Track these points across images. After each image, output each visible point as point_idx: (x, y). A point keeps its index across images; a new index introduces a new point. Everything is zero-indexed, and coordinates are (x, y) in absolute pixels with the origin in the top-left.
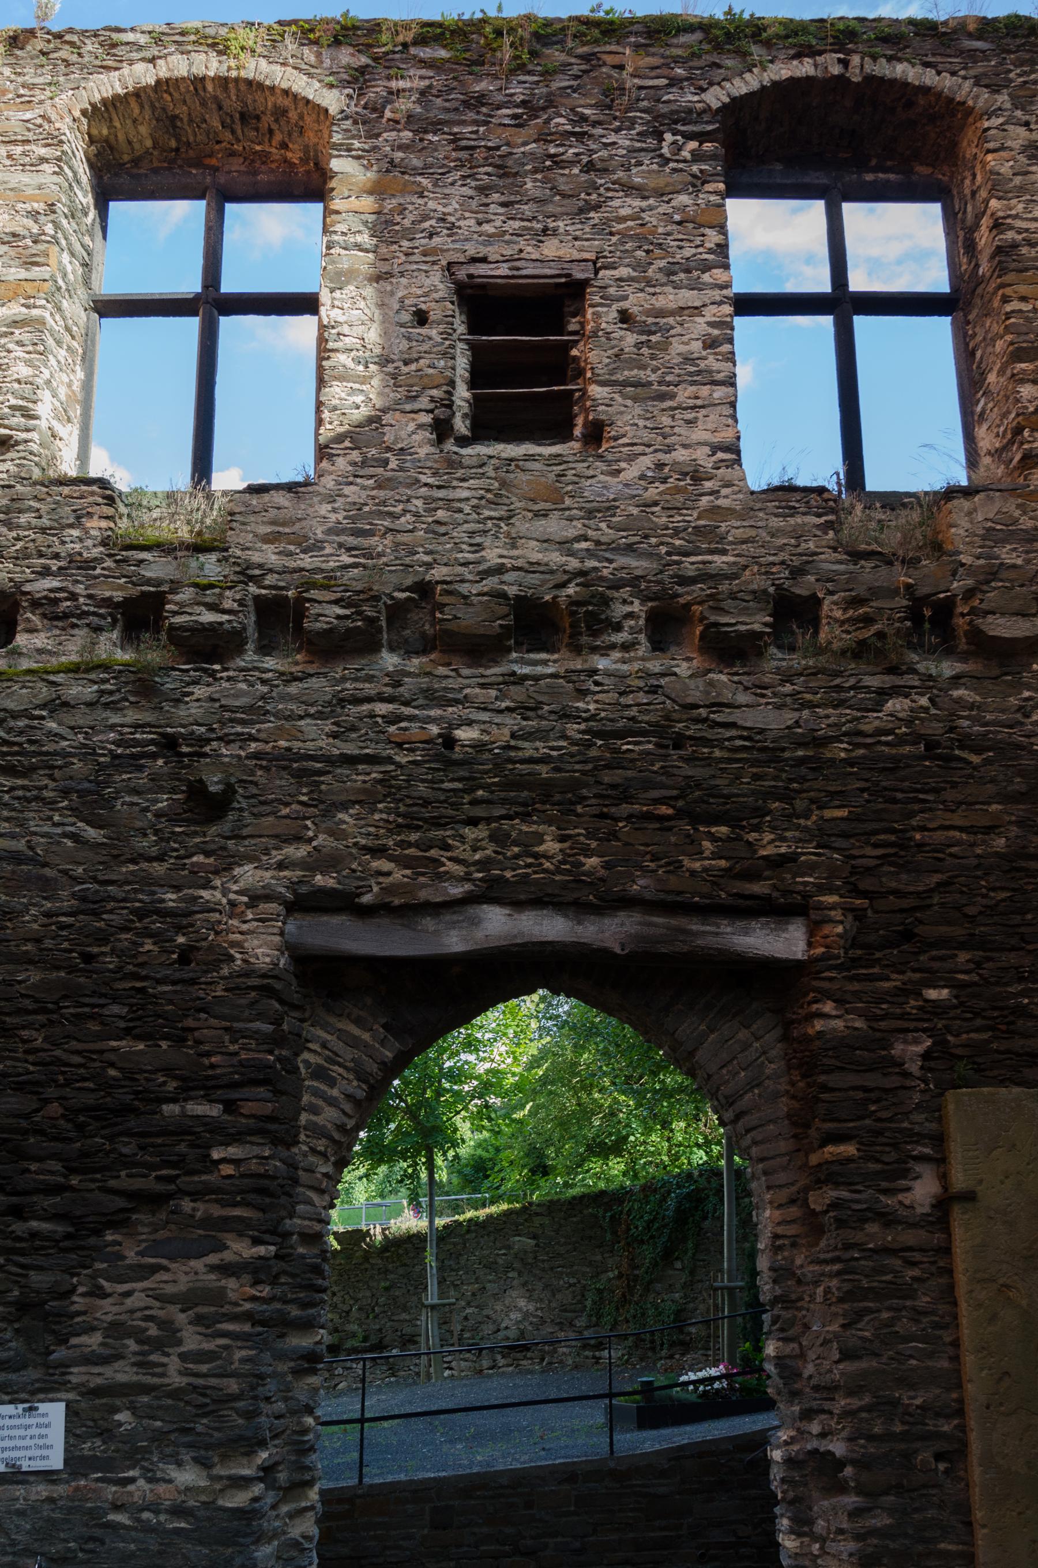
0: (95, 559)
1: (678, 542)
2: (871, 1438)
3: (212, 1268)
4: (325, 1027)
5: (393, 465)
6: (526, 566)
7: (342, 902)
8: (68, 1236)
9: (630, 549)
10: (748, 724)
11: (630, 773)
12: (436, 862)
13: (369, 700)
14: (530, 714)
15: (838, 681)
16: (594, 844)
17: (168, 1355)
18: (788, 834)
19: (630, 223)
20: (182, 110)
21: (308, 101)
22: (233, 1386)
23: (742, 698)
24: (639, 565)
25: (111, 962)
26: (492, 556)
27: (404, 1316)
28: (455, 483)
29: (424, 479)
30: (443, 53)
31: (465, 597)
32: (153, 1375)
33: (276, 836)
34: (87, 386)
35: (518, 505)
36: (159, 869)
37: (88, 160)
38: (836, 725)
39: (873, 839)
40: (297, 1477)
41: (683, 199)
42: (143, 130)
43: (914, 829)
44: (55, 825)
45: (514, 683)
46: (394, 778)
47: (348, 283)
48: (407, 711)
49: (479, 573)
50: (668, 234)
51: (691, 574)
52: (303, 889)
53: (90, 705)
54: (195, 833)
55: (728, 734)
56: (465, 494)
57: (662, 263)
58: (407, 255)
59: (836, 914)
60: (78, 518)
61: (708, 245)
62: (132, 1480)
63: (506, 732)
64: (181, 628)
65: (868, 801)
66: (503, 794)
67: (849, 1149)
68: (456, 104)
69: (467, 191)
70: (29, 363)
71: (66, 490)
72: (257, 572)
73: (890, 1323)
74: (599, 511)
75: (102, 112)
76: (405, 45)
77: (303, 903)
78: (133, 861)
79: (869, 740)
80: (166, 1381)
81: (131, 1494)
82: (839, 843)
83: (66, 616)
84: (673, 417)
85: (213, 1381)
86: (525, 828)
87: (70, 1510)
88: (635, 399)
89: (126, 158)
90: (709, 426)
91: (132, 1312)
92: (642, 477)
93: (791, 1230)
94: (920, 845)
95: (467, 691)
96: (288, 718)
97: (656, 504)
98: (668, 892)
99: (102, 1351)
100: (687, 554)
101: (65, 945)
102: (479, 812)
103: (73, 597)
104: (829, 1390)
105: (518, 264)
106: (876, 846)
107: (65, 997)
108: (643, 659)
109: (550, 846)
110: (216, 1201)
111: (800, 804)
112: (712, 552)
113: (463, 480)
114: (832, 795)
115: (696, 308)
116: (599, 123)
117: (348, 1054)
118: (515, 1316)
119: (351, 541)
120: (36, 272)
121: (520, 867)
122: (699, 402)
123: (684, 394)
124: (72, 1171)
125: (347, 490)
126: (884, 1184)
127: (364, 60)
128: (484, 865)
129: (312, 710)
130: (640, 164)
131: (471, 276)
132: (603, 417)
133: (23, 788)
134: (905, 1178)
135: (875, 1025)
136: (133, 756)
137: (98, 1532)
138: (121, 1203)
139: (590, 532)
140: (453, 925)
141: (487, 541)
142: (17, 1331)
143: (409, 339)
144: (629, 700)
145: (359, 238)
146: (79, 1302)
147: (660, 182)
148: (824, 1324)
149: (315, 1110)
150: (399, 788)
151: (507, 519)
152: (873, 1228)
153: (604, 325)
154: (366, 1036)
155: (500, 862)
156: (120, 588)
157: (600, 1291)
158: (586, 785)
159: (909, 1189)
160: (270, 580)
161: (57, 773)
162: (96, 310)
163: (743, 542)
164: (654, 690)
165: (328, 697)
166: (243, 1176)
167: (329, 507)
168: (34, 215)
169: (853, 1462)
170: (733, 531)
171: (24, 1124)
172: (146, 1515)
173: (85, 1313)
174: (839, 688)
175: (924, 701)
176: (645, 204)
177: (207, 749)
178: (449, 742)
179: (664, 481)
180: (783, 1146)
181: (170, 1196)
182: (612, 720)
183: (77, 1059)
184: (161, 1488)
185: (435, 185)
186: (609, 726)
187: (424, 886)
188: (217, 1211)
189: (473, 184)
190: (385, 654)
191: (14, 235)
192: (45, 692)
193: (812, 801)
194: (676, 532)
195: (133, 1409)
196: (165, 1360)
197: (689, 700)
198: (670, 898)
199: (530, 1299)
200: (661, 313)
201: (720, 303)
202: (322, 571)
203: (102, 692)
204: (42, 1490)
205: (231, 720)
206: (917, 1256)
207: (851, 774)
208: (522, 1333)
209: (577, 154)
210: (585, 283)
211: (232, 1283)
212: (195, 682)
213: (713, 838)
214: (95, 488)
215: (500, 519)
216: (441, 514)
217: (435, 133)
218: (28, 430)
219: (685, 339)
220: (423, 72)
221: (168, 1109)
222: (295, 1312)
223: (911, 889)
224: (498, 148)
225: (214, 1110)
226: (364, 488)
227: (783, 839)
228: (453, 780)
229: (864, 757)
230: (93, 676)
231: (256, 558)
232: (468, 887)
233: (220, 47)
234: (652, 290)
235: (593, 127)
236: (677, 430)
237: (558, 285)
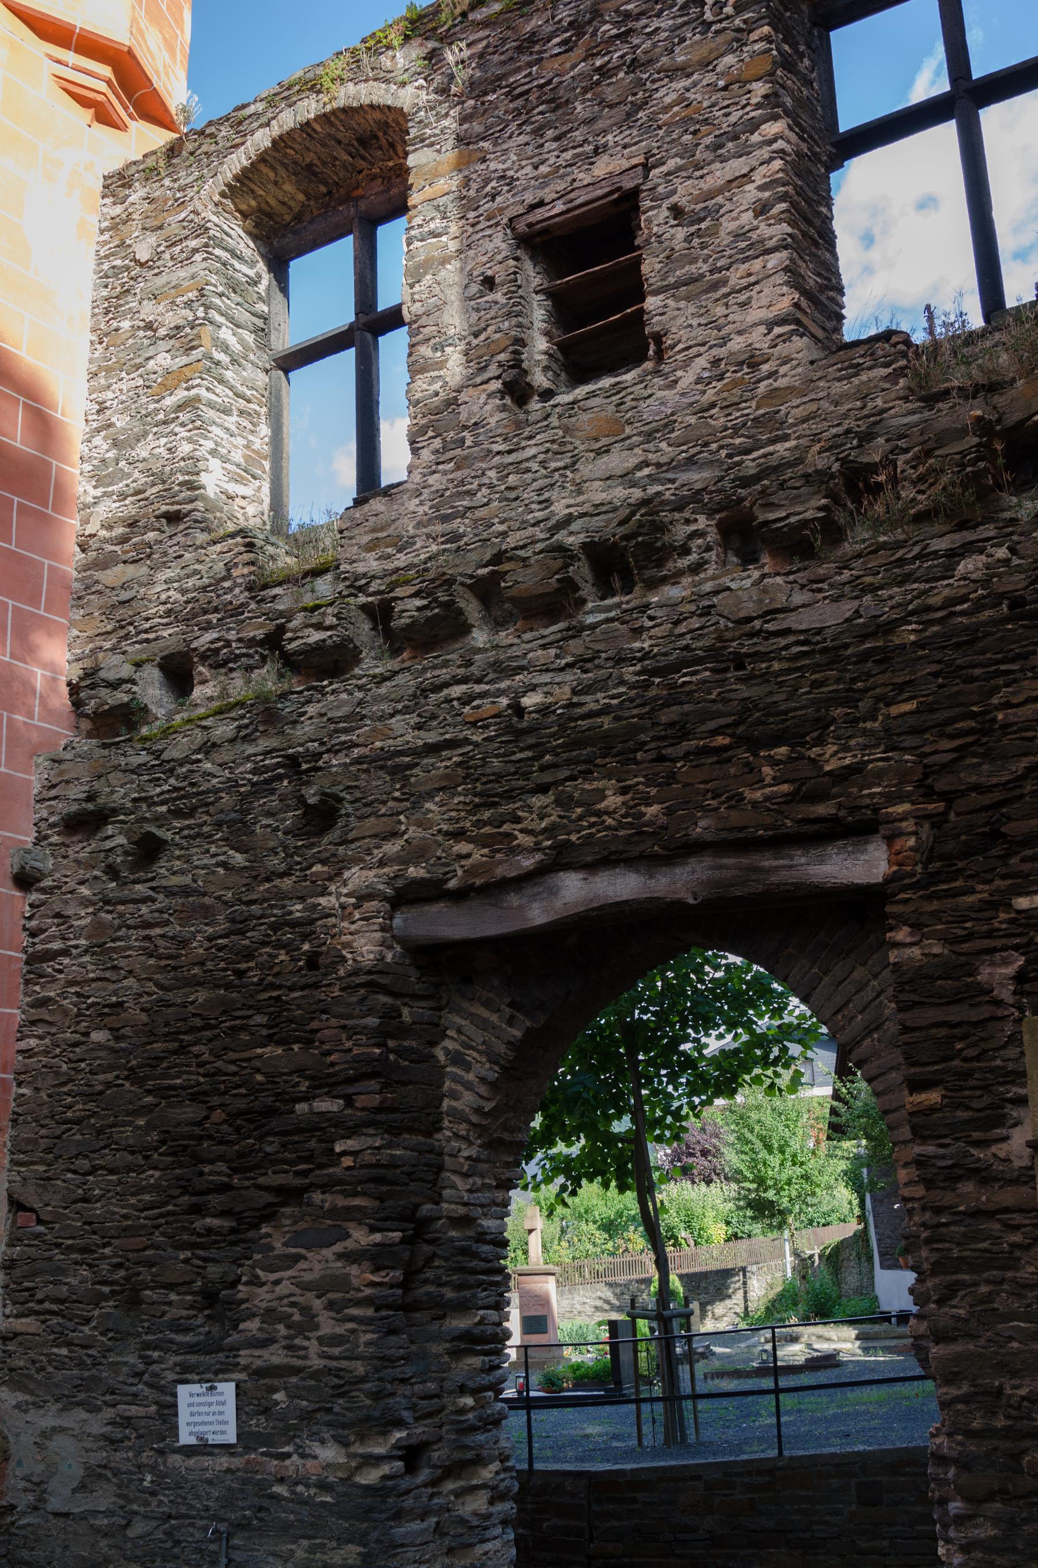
0: (242, 605)
1: (738, 441)
2: (969, 1434)
3: (340, 1256)
4: (460, 1011)
5: (468, 443)
6: (591, 510)
8: (233, 1231)
9: (691, 462)
10: (803, 627)
11: (687, 707)
12: (510, 836)
13: (447, 685)
14: (589, 665)
15: (900, 553)
16: (653, 791)
17: (308, 1339)
18: (853, 742)
19: (676, 109)
20: (310, 157)
21: (389, 107)
22: (360, 1368)
23: (799, 598)
24: (697, 477)
25: (254, 976)
26: (559, 510)
28: (524, 443)
29: (496, 448)
31: (524, 559)
32: (299, 1357)
33: (375, 836)
34: (277, 441)
35: (582, 448)
36: (287, 883)
37: (249, 233)
38: (900, 605)
39: (949, 729)
40: (457, 1455)
41: (729, 59)
42: (288, 187)
43: (997, 708)
44: (214, 856)
45: (573, 637)
46: (472, 758)
47: (425, 273)
48: (478, 688)
49: (550, 529)
50: (713, 105)
51: (752, 472)
52: (399, 883)
53: (232, 741)
54: (313, 844)
55: (783, 642)
56: (531, 452)
57: (708, 140)
58: (473, 225)
59: (908, 825)
60: (228, 570)
61: (754, 101)
62: (288, 1456)
63: (567, 689)
64: (296, 653)
65: (941, 686)
66: (565, 756)
67: (934, 1097)
68: (510, 53)
69: (523, 139)
70: (190, 440)
71: (218, 548)
72: (363, 582)
73: (989, 1298)
74: (657, 431)
75: (242, 186)
76: (464, 15)
77: (406, 896)
78: (268, 879)
79: (940, 614)
80: (309, 1363)
81: (286, 1468)
82: (909, 741)
83: (226, 662)
84: (727, 305)
85: (344, 1364)
86: (587, 786)
87: (245, 1482)
88: (688, 298)
89: (287, 218)
90: (764, 302)
91: (281, 1298)
92: (699, 381)
94: (1005, 726)
95: (531, 655)
96: (381, 719)
97: (713, 405)
98: (731, 830)
99: (261, 1336)
100: (748, 451)
101: (222, 965)
102: (547, 778)
103: (228, 644)
105: (572, 195)
106: (952, 737)
107: (224, 1012)
108: (713, 578)
109: (613, 800)
110: (340, 1192)
111: (864, 705)
112: (773, 441)
113: (530, 438)
114: (901, 688)
115: (744, 176)
116: (642, 14)
117: (479, 1037)
119: (439, 528)
120: (196, 354)
121: (584, 828)
122: (752, 279)
123: (735, 277)
124: (235, 1171)
125: (432, 480)
126: (976, 1135)
127: (431, 45)
128: (550, 831)
129: (400, 706)
130: (683, 40)
131: (530, 225)
132: (657, 329)
133: (189, 827)
134: (1002, 1125)
135: (957, 948)
136: (266, 782)
137: (266, 1503)
138: (269, 1198)
139: (650, 456)
140: (534, 898)
141: (553, 494)
142: (208, 1316)
143: (478, 310)
144: (682, 629)
145: (432, 226)
147: (702, 52)
149: (454, 1095)
150: (476, 768)
151: (572, 466)
152: (967, 1187)
153: (655, 229)
154: (494, 1018)
155: (565, 826)
156: (261, 626)
158: (644, 730)
159: (1005, 1139)
160: (374, 587)
161: (212, 809)
162: (280, 367)
163: (804, 421)
164: (706, 611)
165: (410, 692)
166: (362, 1167)
167: (417, 501)
168: (189, 304)
169: (955, 1462)
170: (794, 411)
171: (197, 1131)
172: (300, 1488)
173: (246, 1301)
174: (901, 562)
175: (1002, 553)
176: (687, 82)
177: (321, 763)
178: (519, 710)
179: (721, 377)
181: (307, 1189)
182: (665, 654)
183: (233, 1068)
184: (310, 1463)
185: (496, 144)
186: (663, 661)
187: (501, 862)
188: (341, 1202)
189: (529, 129)
190: (476, 633)
191: (177, 328)
192: (199, 736)
193: (878, 699)
194: (736, 431)
196: (306, 1343)
197: (742, 614)
198: (732, 836)
200: (710, 195)
201: (771, 159)
202: (415, 566)
203: (239, 728)
204: (224, 1462)
205: (336, 731)
206: (1017, 1218)
207: (921, 658)
209: (622, 57)
210: (634, 194)
211: (354, 1270)
212: (309, 702)
213: (774, 762)
214: (239, 539)
215: (565, 468)
216: (512, 480)
217: (494, 91)
218: (192, 501)
219: (734, 214)
220: (481, 34)
221: (301, 1107)
222: (449, 1294)
223: (995, 780)
224: (549, 82)
226: (445, 473)
227: (846, 749)
228: (522, 750)
229: (935, 635)
230: (233, 714)
231: (361, 568)
232: (539, 856)
233: (312, 86)
234: (698, 173)
235: (637, 20)
236: (731, 318)
237: (615, 201)
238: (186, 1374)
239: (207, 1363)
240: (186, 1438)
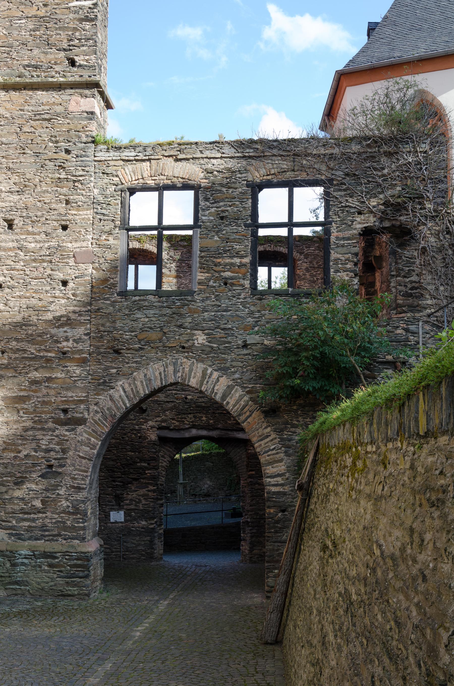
7: (167, 428)
12: (184, 421)
22: (151, 509)
27: (172, 484)
30: (186, 244)
36: (134, 422)
48: (178, 392)
67: (254, 473)
77: (160, 428)
93: (245, 485)
102: (191, 412)
104: (248, 511)
109: (204, 418)
117: (168, 453)
118: (206, 486)
128: (192, 422)
146: (125, 496)
148: (248, 501)
149: (162, 463)
152: (257, 485)
157: (231, 480)
178: (186, 398)
180: (245, 470)
181: (139, 479)
195: (134, 512)
199: (211, 481)
204: (121, 525)
208: (208, 491)
211: (150, 493)
221: (138, 464)
222: (159, 497)
225: (146, 465)
238: (112, 509)
239: (120, 508)
240: (112, 520)
